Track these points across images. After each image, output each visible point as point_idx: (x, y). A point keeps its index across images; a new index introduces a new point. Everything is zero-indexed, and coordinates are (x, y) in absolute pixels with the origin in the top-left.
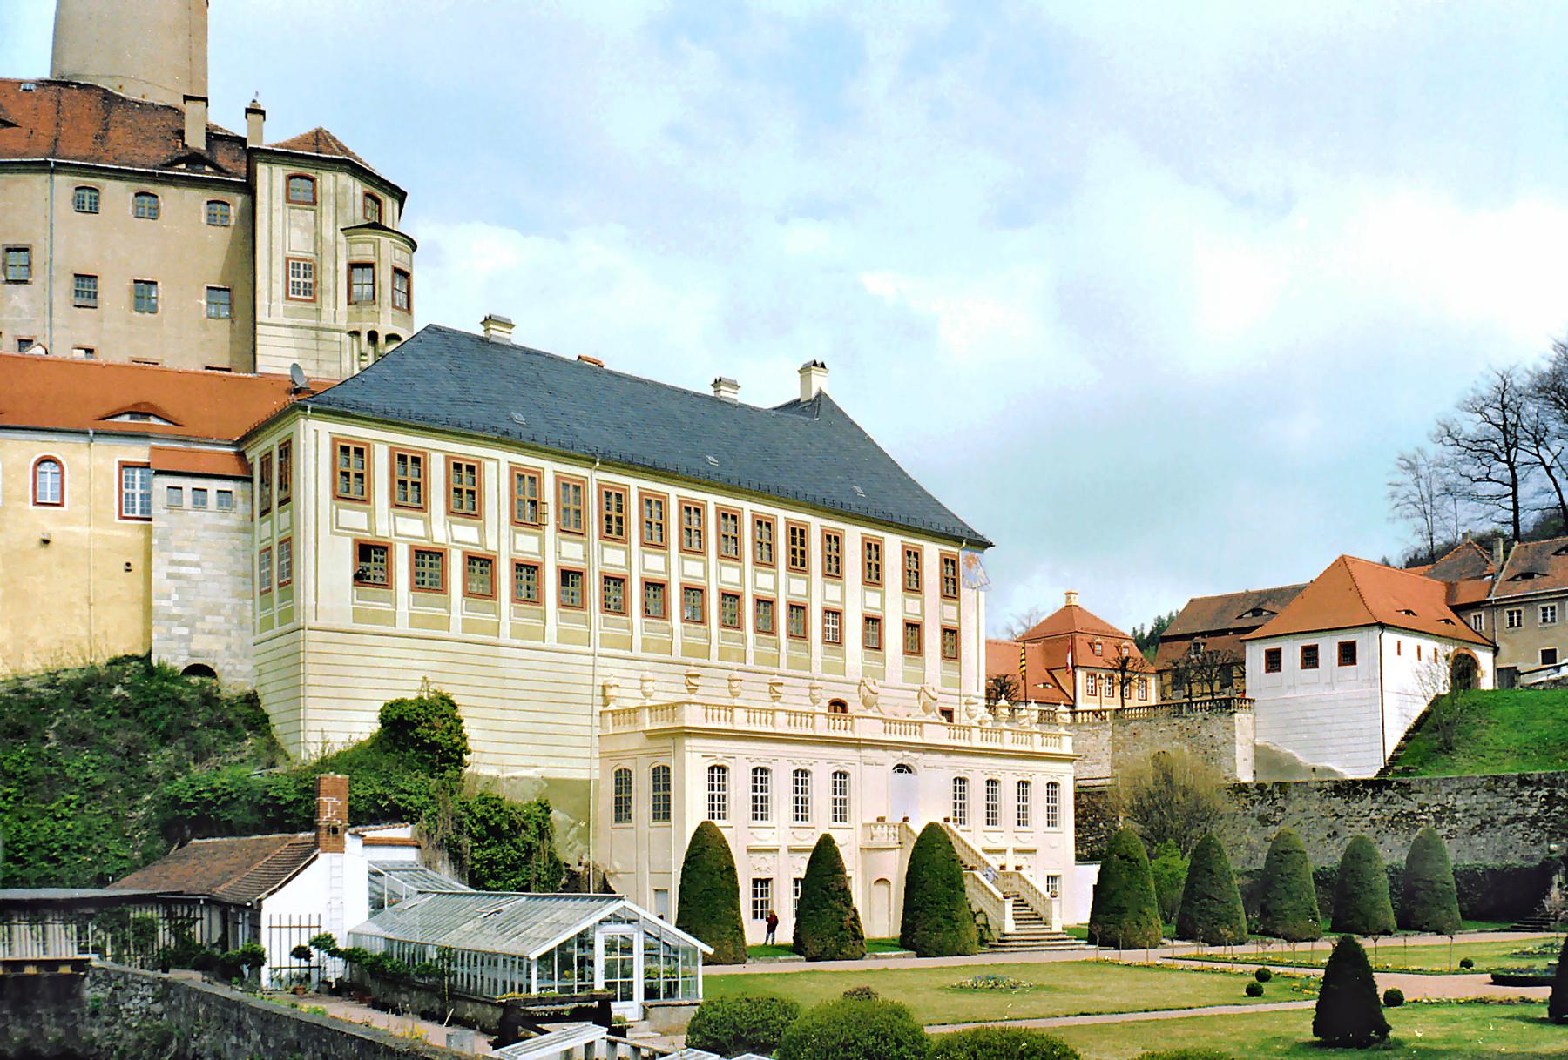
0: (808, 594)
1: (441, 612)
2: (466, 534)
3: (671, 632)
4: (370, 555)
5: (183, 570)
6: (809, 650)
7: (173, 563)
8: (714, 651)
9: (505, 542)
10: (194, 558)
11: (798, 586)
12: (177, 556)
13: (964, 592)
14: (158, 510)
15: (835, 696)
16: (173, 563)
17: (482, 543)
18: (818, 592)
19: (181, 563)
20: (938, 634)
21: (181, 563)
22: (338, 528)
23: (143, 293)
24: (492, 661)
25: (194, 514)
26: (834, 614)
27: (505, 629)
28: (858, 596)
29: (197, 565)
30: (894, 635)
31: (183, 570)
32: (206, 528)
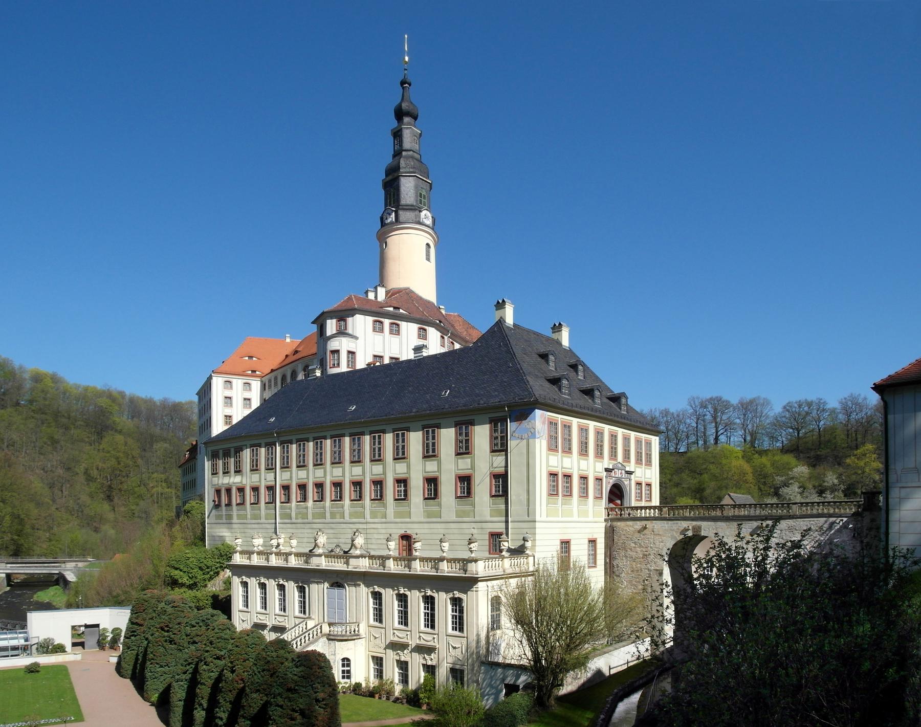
0: (384, 473)
3: (307, 508)
4: (218, 492)
6: (385, 506)
8: (328, 515)
9: (248, 480)
11: (378, 469)
13: (512, 444)
15: (402, 532)
17: (241, 482)
18: (392, 470)
20: (488, 479)
24: (246, 530)
26: (402, 482)
27: (249, 516)
28: (420, 467)
30: (448, 488)
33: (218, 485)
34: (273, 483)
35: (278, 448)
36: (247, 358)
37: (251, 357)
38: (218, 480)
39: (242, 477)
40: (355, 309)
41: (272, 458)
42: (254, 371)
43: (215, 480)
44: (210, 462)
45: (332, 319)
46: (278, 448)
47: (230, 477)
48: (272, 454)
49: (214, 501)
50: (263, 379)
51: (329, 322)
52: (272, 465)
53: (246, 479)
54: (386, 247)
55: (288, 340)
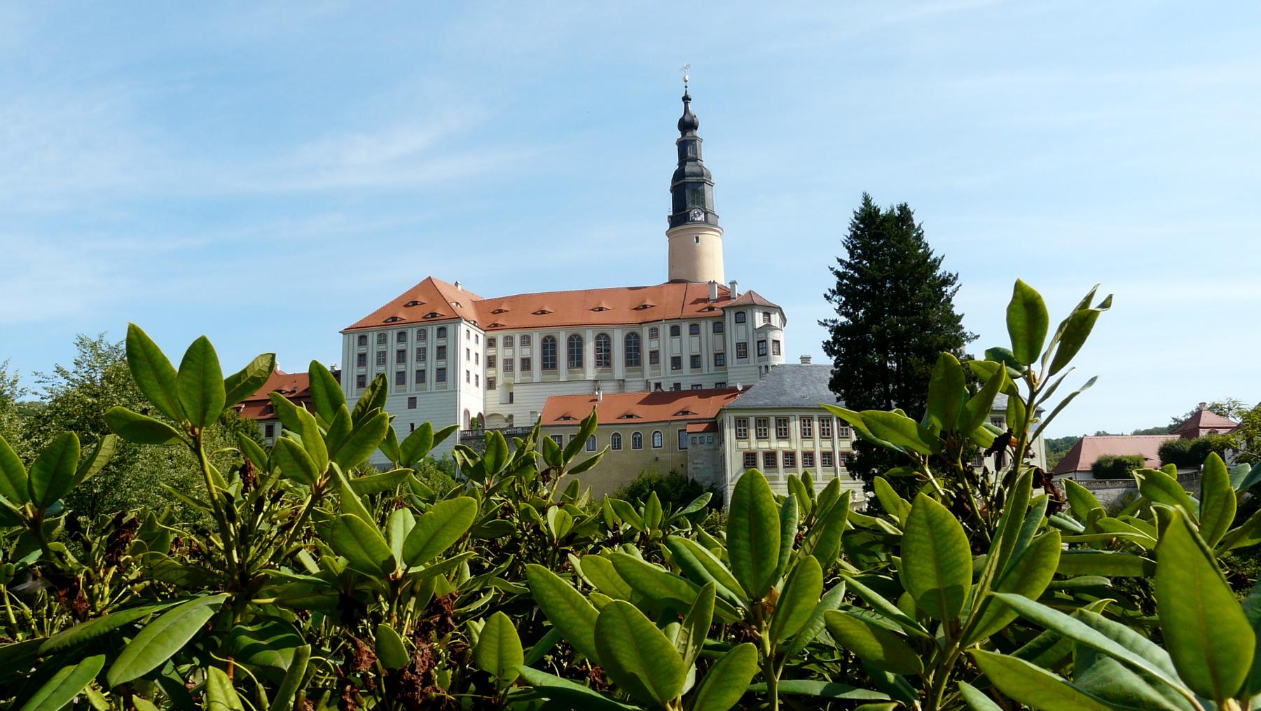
1: (776, 474)
2: (784, 445)
4: (750, 459)
5: (698, 466)
7: (694, 464)
10: (701, 462)
12: (695, 461)
14: (689, 447)
16: (694, 464)
19: (696, 464)
21: (696, 464)
22: (738, 449)
23: (695, 361)
25: (700, 446)
29: (702, 463)
31: (698, 466)
32: (704, 451)
33: (749, 448)
34: (831, 450)
35: (835, 423)
36: (455, 304)
37: (457, 303)
38: (749, 444)
39: (790, 442)
40: (780, 308)
41: (828, 430)
42: (475, 322)
43: (744, 445)
44: (733, 431)
45: (759, 312)
46: (835, 423)
47: (769, 442)
48: (828, 425)
49: (745, 465)
50: (491, 334)
51: (757, 314)
52: (829, 434)
53: (798, 445)
54: (697, 241)
55: (459, 287)
